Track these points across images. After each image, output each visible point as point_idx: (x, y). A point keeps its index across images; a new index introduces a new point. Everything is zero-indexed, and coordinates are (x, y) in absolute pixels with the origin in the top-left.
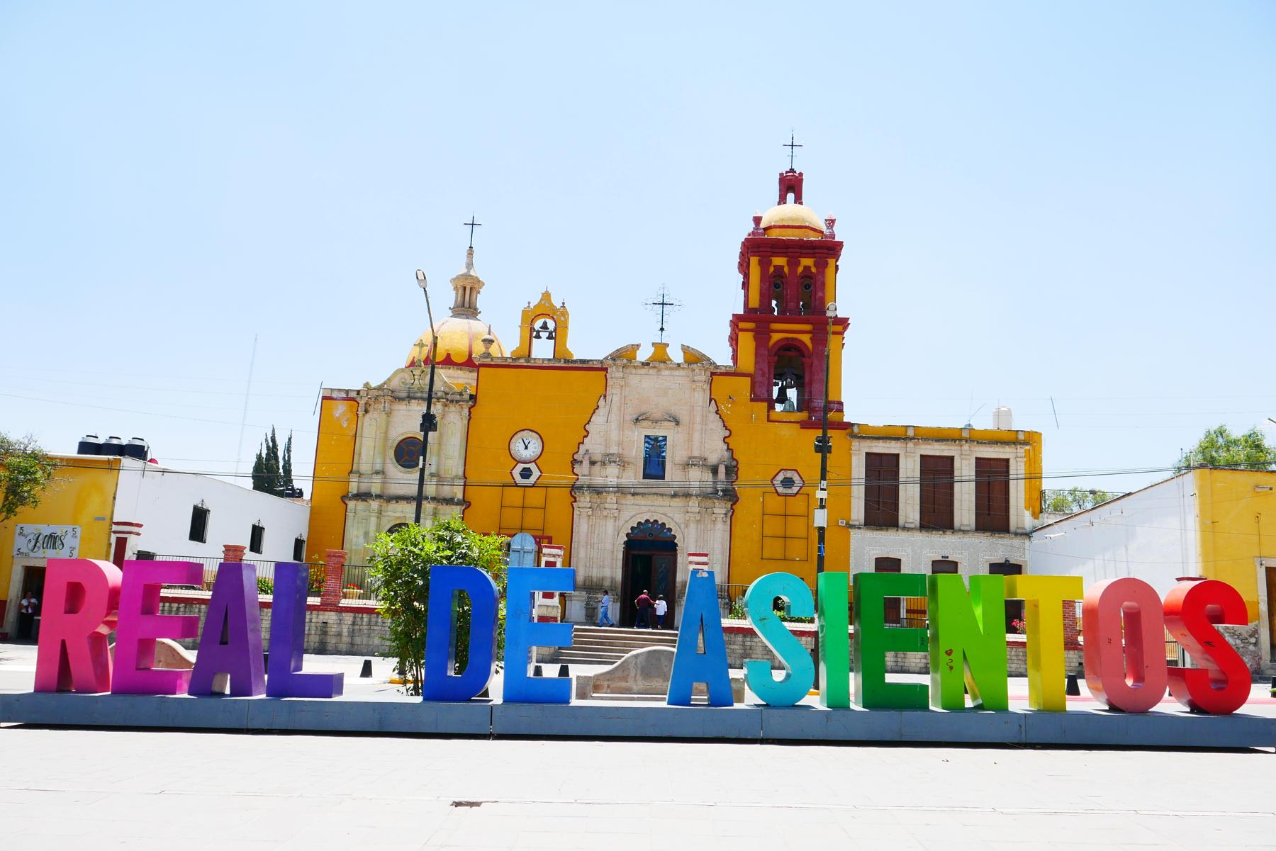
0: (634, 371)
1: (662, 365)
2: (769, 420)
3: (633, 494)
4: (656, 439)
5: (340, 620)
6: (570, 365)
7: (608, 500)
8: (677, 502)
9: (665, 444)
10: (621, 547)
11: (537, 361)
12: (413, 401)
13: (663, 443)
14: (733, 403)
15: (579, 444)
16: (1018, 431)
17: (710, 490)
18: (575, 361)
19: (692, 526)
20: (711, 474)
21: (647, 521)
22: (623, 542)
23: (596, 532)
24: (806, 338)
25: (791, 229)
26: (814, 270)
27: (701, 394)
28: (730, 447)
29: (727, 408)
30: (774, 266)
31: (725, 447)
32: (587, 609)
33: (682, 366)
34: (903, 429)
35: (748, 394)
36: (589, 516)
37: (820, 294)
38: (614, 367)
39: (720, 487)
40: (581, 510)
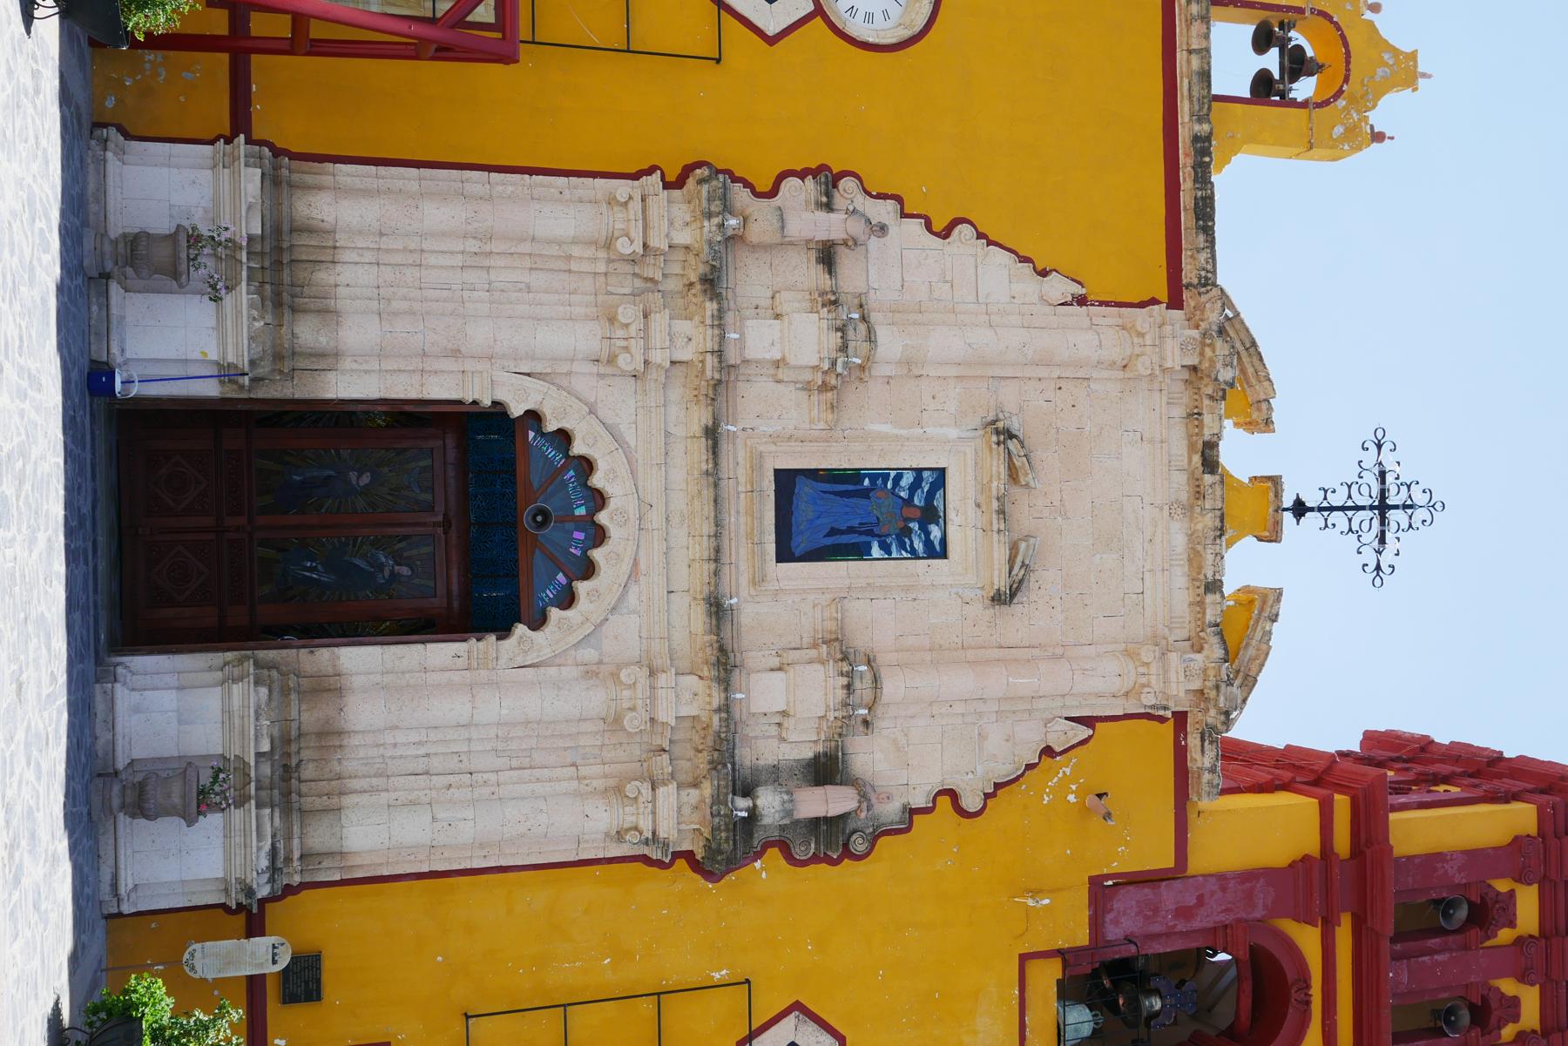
0: (1179, 412)
1: (1209, 521)
2: (1024, 958)
3: (712, 434)
4: (931, 515)
6: (1185, 161)
7: (683, 327)
8: (691, 621)
9: (915, 556)
10: (476, 390)
11: (1197, 27)
13: (919, 546)
14: (1084, 811)
15: (898, 199)
17: (747, 756)
19: (595, 700)
20: (810, 755)
21: (598, 499)
22: (501, 396)
23: (539, 280)
26: (1508, 1032)
27: (1117, 685)
28: (915, 817)
29: (1062, 788)
30: (1512, 894)
31: (920, 801)
32: (172, 238)
33: (1210, 598)
35: (1116, 867)
36: (609, 244)
38: (1195, 333)
39: (769, 802)
40: (636, 205)
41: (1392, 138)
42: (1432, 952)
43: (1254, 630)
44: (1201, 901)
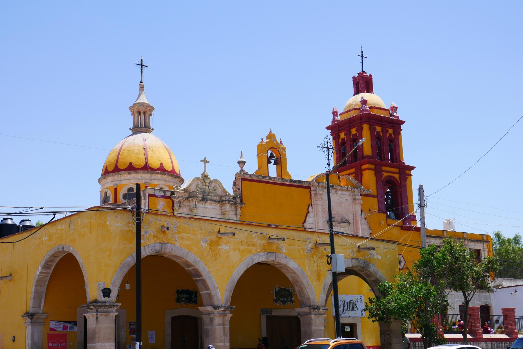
1: (339, 188)
5: (487, 346)
12: (209, 202)
16: (483, 235)
24: (397, 176)
25: (381, 110)
26: (393, 136)
29: (369, 216)
33: (349, 189)
34: (442, 232)
37: (397, 151)
42: (383, 150)
43: (350, 180)
44: (380, 194)
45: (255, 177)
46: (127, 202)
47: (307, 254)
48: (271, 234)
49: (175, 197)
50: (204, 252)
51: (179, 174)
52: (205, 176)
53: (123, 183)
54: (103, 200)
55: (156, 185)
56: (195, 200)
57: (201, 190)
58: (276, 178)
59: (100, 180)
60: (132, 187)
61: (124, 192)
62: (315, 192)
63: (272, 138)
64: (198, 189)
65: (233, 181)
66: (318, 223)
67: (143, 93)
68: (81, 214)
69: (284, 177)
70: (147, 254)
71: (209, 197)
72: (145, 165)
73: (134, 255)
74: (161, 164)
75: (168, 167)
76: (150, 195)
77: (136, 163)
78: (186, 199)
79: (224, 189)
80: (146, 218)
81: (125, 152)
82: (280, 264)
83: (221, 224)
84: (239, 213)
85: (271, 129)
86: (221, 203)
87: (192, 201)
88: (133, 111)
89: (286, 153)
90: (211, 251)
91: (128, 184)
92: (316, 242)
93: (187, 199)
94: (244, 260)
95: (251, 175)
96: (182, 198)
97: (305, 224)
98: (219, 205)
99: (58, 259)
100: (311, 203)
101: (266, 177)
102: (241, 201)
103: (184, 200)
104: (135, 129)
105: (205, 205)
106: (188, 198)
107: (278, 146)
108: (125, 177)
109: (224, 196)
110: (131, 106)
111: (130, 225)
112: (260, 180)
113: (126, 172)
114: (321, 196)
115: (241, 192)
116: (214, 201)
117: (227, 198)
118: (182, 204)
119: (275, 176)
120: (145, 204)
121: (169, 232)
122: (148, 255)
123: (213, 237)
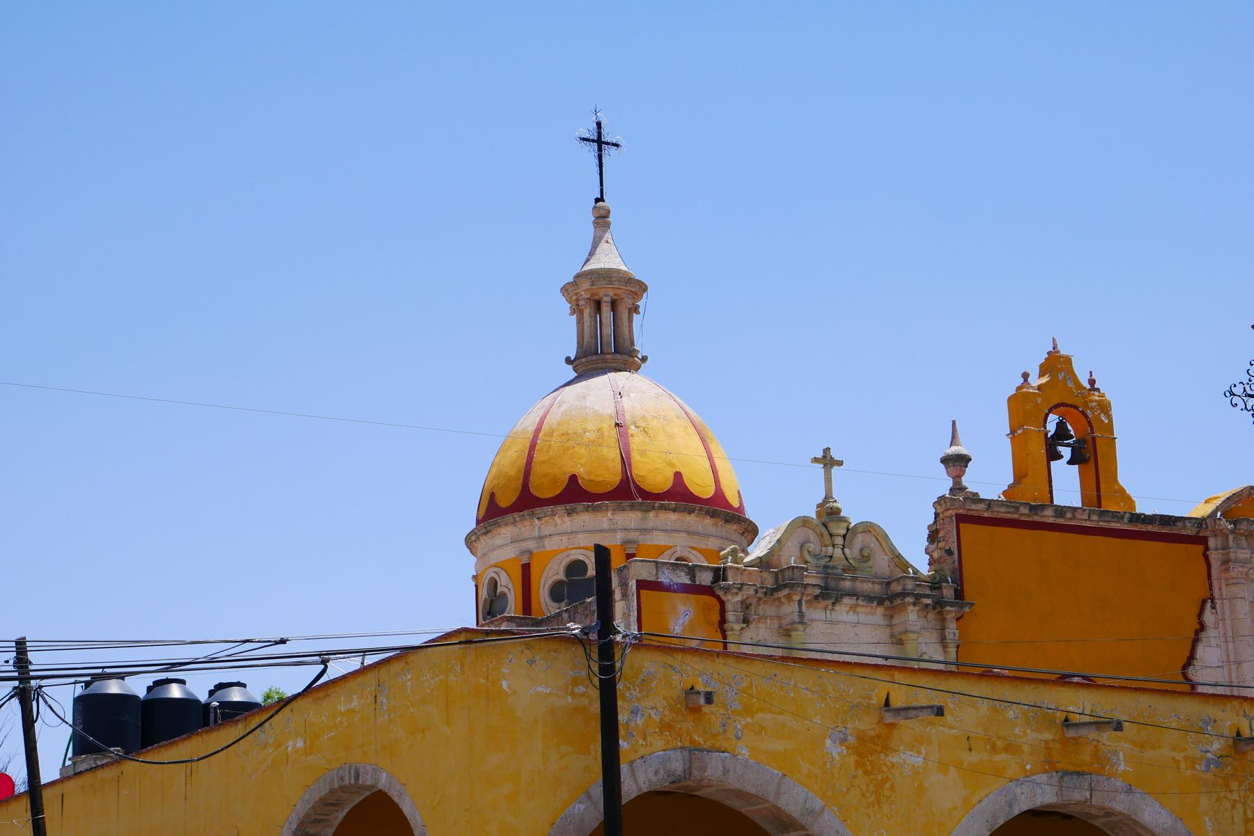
6: (1143, 528)
12: (846, 600)
18: (1151, 519)
41: (1091, 372)
45: (1003, 510)
46: (566, 611)
47: (1205, 777)
48: (1071, 709)
49: (727, 590)
50: (837, 775)
51: (741, 509)
52: (829, 513)
53: (551, 545)
54: (484, 606)
55: (661, 550)
56: (797, 598)
57: (818, 559)
58: (1080, 511)
59: (473, 538)
60: (581, 558)
61: (555, 578)
62: (1223, 555)
63: (1060, 370)
64: (808, 558)
65: (929, 527)
66: (1239, 663)
67: (608, 236)
68: (413, 658)
69: (1107, 505)
70: (640, 789)
71: (847, 584)
72: (622, 481)
73: (598, 791)
74: (678, 475)
75: (702, 486)
76: (642, 585)
77: (592, 478)
78: (765, 594)
79: (899, 556)
80: (631, 664)
81: (554, 439)
82: (1109, 814)
83: (893, 676)
84: (952, 636)
85: (1054, 339)
86: (887, 603)
87: (789, 602)
88: (575, 298)
89: (1111, 421)
90: (860, 772)
91: (567, 549)
92: (1238, 734)
93: (769, 593)
94: (980, 801)
95: (990, 503)
96: (751, 592)
97: (1190, 670)
98: (880, 610)
99: (342, 814)
100: (1212, 595)
101: (1043, 507)
102: (959, 594)
103: (760, 599)
104: (584, 360)
105: (833, 612)
106: (773, 591)
107: (1084, 398)
108: (556, 525)
109: (898, 580)
110: (568, 283)
111: (580, 689)
112: (1023, 518)
113: (560, 508)
114: (1246, 570)
115: (956, 563)
116: (865, 596)
117: (910, 585)
118: (753, 610)
119: (1077, 503)
120: (626, 616)
121: (714, 710)
122: (645, 790)
123: (867, 724)
